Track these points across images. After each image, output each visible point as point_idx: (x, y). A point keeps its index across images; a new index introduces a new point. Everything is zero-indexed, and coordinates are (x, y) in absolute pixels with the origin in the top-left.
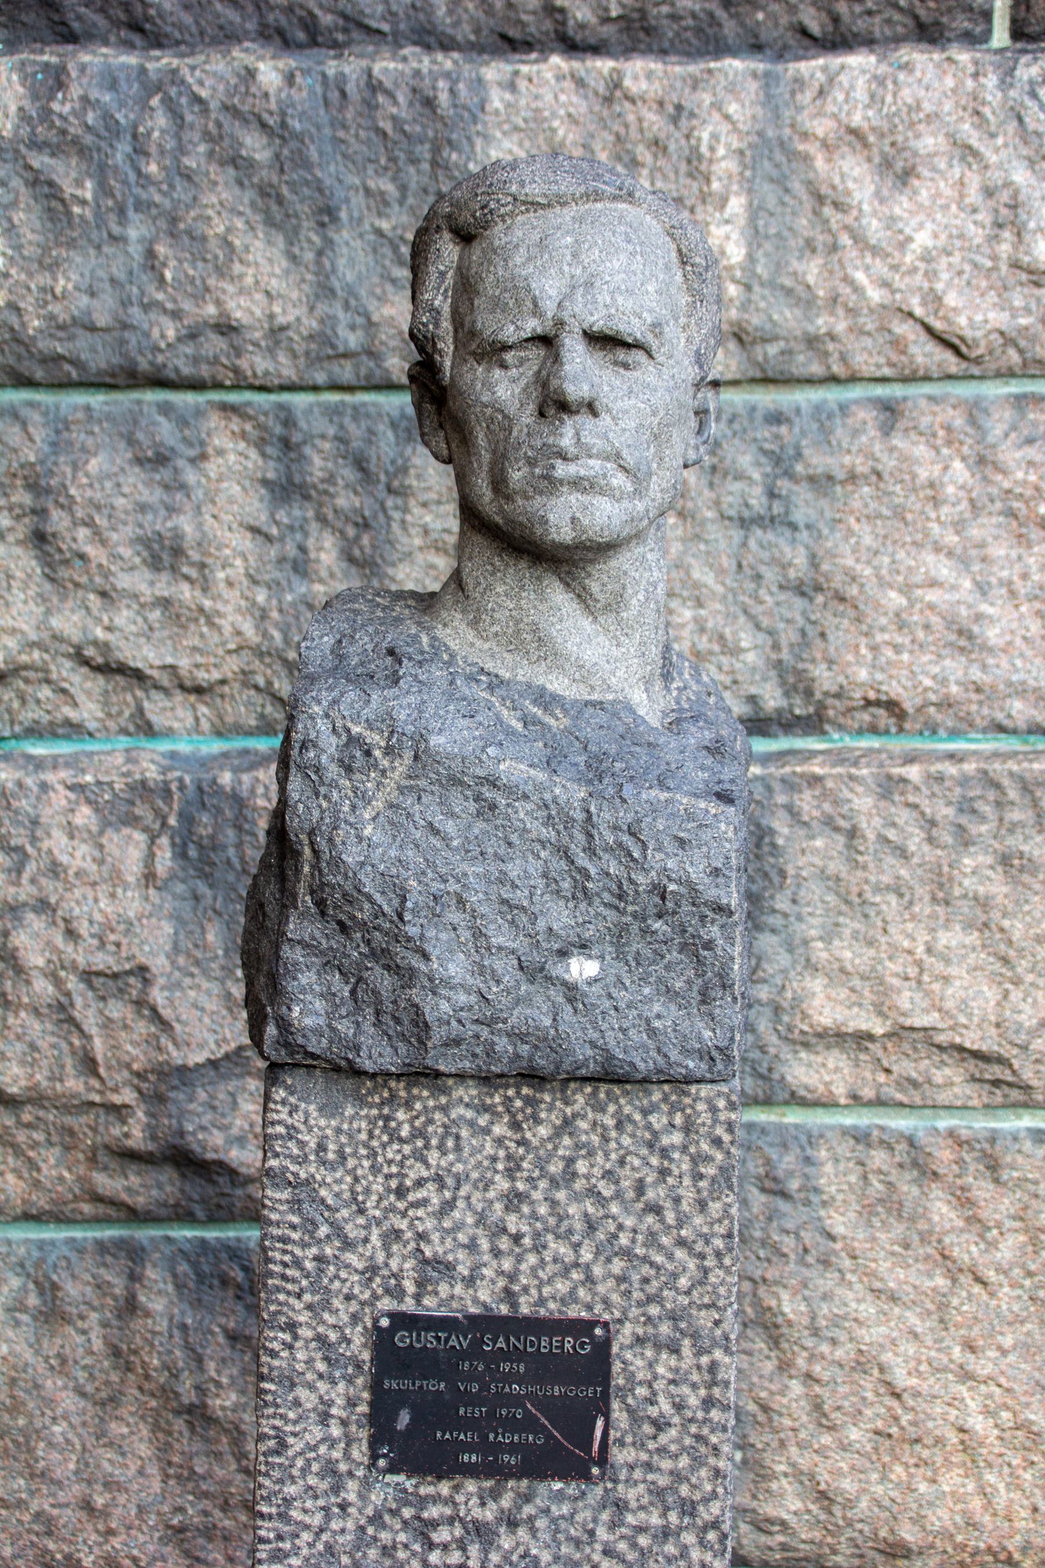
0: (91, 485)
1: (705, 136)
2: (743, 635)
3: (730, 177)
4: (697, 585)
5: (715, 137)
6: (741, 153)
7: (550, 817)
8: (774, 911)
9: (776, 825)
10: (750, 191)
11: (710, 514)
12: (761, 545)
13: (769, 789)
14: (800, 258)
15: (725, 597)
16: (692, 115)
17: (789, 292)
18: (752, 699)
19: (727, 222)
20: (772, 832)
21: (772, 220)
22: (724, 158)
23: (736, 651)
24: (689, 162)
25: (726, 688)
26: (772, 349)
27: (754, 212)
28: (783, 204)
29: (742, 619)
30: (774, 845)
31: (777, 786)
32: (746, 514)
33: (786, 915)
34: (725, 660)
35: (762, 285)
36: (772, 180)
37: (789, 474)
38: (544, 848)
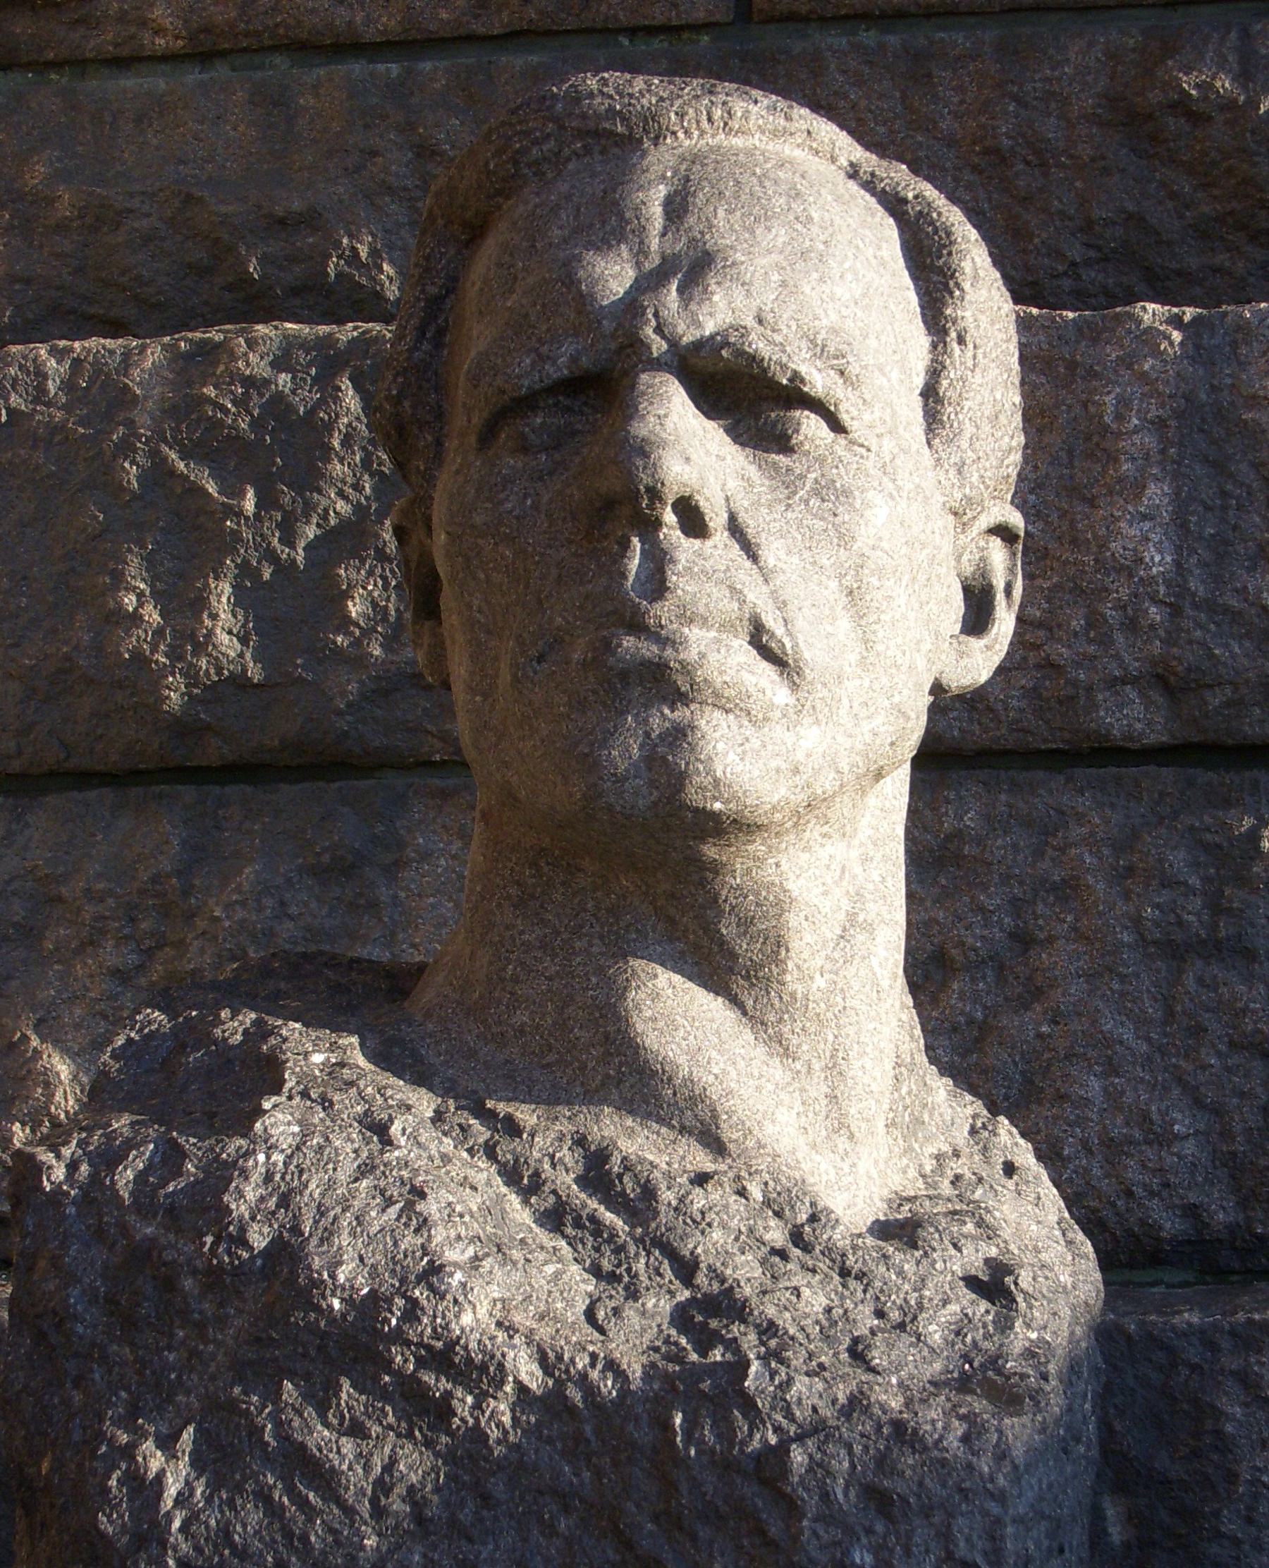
0: (243, 903)
1: (1109, 399)
2: (1177, 1115)
3: (1147, 457)
4: (1109, 1041)
5: (1124, 402)
6: (1160, 424)
7: (579, 1438)
8: (1219, 1535)
9: (1223, 1403)
10: (1176, 476)
11: (1126, 937)
12: (1200, 981)
13: (1213, 1347)
14: (1252, 569)
15: (1149, 1059)
16: (1092, 374)
17: (1236, 616)
18: (1192, 1211)
19: (1144, 517)
20: (1218, 1414)
21: (1209, 515)
22: (1136, 431)
23: (1165, 1139)
24: (1088, 439)
25: (1152, 1194)
26: (1215, 700)
27: (1181, 506)
28: (1224, 494)
29: (1176, 1092)
30: (1218, 1433)
31: (1225, 1344)
32: (1178, 936)
33: (1237, 1542)
34: (1150, 1153)
35: (1196, 606)
36: (1206, 460)
37: (1242, 880)
38: (567, 1510)
